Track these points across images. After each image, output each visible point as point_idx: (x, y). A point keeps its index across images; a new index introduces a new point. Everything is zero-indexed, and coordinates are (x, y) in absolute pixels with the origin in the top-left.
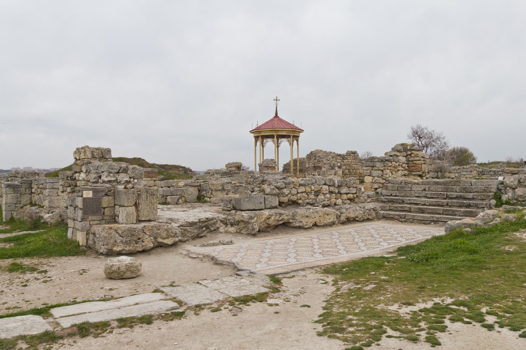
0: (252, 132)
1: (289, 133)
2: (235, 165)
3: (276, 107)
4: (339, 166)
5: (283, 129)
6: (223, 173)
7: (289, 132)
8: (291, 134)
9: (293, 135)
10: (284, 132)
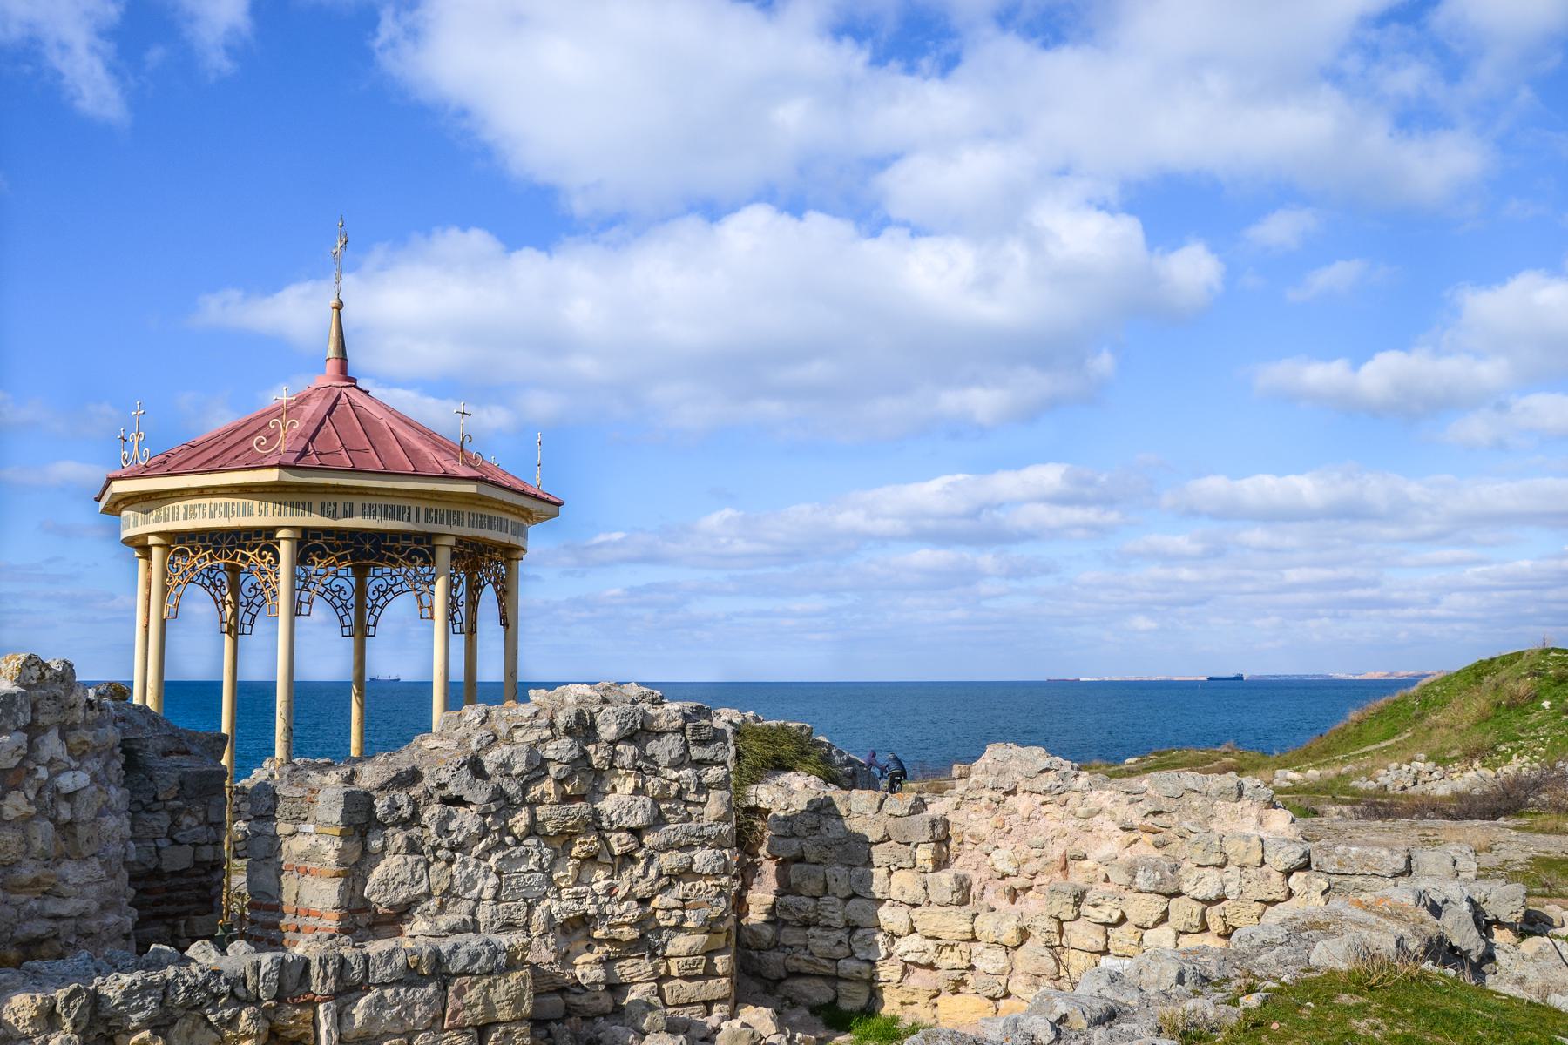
9: (460, 540)
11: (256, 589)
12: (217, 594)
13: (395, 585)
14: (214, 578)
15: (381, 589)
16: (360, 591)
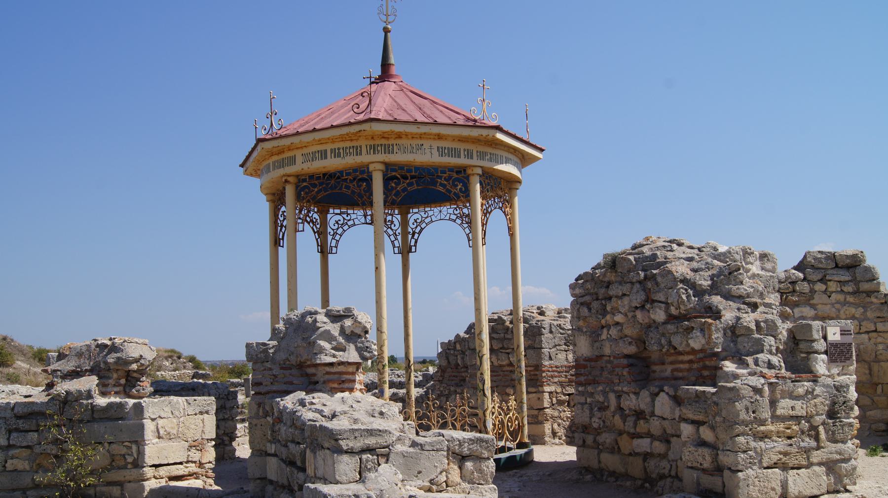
1: (456, 153)
3: (386, 31)
4: (835, 345)
5: (424, 129)
6: (18, 417)
7: (462, 146)
8: (475, 162)
10: (427, 144)
11: (338, 224)
12: (314, 227)
13: (427, 217)
14: (312, 216)
15: (418, 221)
16: (404, 223)
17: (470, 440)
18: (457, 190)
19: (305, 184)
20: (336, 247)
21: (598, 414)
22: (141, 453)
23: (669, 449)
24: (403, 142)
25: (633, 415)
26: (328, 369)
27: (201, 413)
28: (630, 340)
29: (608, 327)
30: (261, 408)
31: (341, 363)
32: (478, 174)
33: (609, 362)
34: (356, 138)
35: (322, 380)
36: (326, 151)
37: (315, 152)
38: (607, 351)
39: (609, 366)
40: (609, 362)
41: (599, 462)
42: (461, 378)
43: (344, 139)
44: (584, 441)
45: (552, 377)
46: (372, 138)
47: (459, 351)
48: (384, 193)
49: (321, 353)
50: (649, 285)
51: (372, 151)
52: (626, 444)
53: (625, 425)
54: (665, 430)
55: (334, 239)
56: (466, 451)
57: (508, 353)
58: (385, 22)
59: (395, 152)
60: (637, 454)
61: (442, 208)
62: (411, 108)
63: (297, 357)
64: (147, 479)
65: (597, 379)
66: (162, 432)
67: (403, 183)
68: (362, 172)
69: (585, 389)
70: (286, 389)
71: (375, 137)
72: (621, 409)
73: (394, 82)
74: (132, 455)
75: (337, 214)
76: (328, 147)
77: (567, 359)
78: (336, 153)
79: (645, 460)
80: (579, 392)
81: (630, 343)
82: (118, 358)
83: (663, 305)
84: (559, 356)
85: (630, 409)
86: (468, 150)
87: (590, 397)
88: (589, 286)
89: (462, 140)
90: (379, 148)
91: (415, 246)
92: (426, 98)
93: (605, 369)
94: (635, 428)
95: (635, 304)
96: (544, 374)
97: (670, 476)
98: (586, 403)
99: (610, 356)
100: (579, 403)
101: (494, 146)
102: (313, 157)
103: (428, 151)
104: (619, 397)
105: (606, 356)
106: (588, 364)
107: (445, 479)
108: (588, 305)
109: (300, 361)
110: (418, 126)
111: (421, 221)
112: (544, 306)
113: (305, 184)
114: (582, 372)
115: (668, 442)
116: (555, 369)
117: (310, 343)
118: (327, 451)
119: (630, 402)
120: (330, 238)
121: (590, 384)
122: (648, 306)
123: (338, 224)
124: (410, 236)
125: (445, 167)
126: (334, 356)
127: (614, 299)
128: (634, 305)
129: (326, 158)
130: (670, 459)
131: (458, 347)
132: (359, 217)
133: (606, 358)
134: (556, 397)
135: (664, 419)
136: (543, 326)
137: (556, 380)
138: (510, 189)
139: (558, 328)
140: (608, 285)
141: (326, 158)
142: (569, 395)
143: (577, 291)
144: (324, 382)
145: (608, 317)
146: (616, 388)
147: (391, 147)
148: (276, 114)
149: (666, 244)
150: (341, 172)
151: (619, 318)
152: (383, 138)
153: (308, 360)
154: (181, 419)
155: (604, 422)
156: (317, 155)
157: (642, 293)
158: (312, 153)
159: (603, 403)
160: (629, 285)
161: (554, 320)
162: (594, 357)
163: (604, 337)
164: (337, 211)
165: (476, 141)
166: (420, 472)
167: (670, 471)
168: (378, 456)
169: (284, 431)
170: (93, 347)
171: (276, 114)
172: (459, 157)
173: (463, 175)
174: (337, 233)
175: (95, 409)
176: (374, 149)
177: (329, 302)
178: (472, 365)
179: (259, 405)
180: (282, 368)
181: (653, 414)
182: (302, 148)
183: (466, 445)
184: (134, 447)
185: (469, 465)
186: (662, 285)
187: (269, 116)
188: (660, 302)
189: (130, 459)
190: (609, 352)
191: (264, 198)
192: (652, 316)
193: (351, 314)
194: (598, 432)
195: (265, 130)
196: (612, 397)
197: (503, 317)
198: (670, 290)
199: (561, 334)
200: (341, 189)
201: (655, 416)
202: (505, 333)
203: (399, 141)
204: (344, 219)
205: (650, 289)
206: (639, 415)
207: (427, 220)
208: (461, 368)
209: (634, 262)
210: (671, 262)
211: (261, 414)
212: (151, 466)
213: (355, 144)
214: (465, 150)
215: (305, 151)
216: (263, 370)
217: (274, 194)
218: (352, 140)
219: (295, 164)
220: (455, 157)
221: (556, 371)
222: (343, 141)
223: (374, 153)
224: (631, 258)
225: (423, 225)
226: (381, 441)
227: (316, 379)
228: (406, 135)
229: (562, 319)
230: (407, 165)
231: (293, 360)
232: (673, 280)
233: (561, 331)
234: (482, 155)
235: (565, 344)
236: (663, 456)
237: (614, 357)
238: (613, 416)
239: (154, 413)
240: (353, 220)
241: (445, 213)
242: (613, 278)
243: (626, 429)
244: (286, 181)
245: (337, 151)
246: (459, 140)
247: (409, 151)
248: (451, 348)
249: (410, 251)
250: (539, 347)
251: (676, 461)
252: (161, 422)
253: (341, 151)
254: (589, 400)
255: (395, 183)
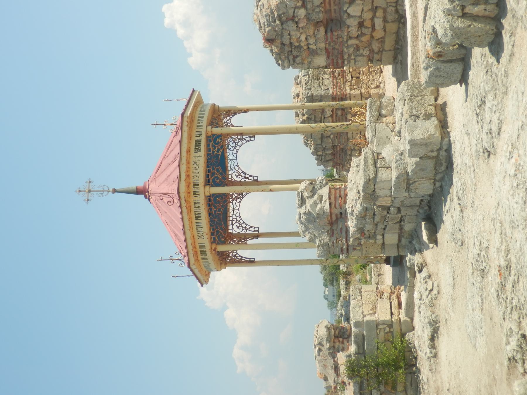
0: (202, 280)
1: (198, 142)
2: (325, 351)
3: (115, 191)
5: (184, 160)
7: (194, 138)
8: (203, 130)
10: (192, 160)
11: (239, 226)
15: (237, 175)
17: (370, 111)
18: (221, 142)
19: (217, 238)
20: (254, 228)
21: (361, 51)
22: (384, 323)
23: (380, 7)
24: (191, 174)
25: (361, 29)
26: (333, 206)
27: (360, 292)
28: (316, 31)
29: (308, 44)
30: (356, 248)
31: (330, 198)
32: (211, 129)
33: (329, 44)
34: (189, 203)
35: (339, 210)
36: (197, 223)
37: (197, 230)
38: (323, 45)
39: (332, 44)
40: (329, 44)
41: (390, 50)
42: (341, 151)
43: (190, 211)
44: (378, 60)
45: (340, 88)
46: (189, 193)
47: (322, 153)
48: (224, 186)
49: (323, 209)
50: (284, 19)
51: (197, 193)
52: (379, 34)
53: (367, 34)
54: (370, 10)
55: (249, 229)
56: (376, 113)
57: (324, 118)
58: (108, 192)
59: (198, 179)
60: (384, 26)
61: (228, 159)
62: (168, 172)
63: (326, 225)
64: (400, 319)
65: (340, 52)
66: (371, 312)
67: (217, 174)
68: (210, 200)
69: (346, 60)
70: (345, 232)
71: (189, 191)
72: (357, 37)
73: (149, 185)
74: (385, 329)
75: (233, 227)
76: (194, 221)
77: (328, 79)
78: (198, 216)
79: (388, 22)
80: (348, 63)
81: (318, 31)
82: (327, 340)
83: (296, 10)
84: (326, 83)
85: (358, 31)
86: (196, 134)
87: (351, 57)
88: (283, 56)
89: (190, 138)
90: (196, 189)
91: (253, 177)
92: (161, 163)
93: (334, 47)
94: (369, 28)
95: (295, 27)
96: (338, 93)
97: (396, 6)
98: (355, 59)
99: (326, 44)
100: (355, 63)
101: (193, 119)
102: (200, 231)
103: (197, 159)
104: (351, 38)
105: (326, 46)
106: (331, 58)
107: (391, 124)
108: (295, 57)
109: (328, 224)
110: (182, 164)
111: (237, 172)
112: (293, 94)
113: (217, 238)
114: (336, 61)
115: (376, 7)
116: (335, 87)
117: (318, 217)
118: (376, 186)
119: (354, 31)
120: (248, 232)
121: (343, 56)
122: (296, 20)
123: (239, 226)
124: (247, 180)
125: (207, 149)
126: (325, 201)
127: (292, 41)
128: (296, 28)
129: (201, 223)
130: (386, 6)
131: (320, 153)
132: (235, 213)
133: (327, 46)
134: (354, 86)
135: (363, 10)
136: (306, 94)
137: (342, 86)
138: (219, 111)
139: (308, 84)
140: (283, 44)
141: (201, 223)
142: (352, 77)
143: (286, 64)
144: (341, 208)
145: (302, 44)
146: (345, 40)
147: (194, 181)
148: (172, 257)
149: (259, 9)
150: (210, 214)
151: (303, 38)
152: (189, 186)
153: (328, 219)
154: (364, 302)
155: (366, 48)
156: (199, 229)
157: (289, 23)
158: (198, 232)
159: (354, 48)
160: (284, 31)
161: (302, 87)
162: (326, 54)
163: (314, 47)
164: (231, 227)
165: (190, 128)
166: (387, 137)
167: (393, 6)
168: (378, 159)
169: (369, 227)
170: (320, 358)
171: (172, 257)
172: (201, 140)
173: (212, 138)
174: (245, 227)
175: (357, 352)
176: (196, 192)
177: (290, 232)
178: (332, 142)
179: (354, 249)
180: (333, 236)
181: (360, 17)
182: (194, 239)
183: (373, 113)
184: (380, 327)
185: (384, 112)
186: (285, 11)
187: (173, 262)
188: (294, 12)
189: (388, 330)
190: (323, 44)
191: (223, 270)
192: (303, 17)
193: (301, 192)
194: (372, 51)
195: (181, 264)
196: (350, 42)
197: (300, 121)
198: (288, 6)
199: (312, 82)
200: (220, 214)
201: (361, 15)
202: (311, 120)
203: (191, 176)
204: (236, 223)
205: (286, 18)
206: (361, 25)
207: (237, 169)
208: (334, 151)
209: (270, 28)
210: (270, 6)
211: (359, 248)
212: (392, 317)
213: (192, 204)
214: (196, 136)
215: (196, 237)
216: (334, 247)
217: (221, 264)
218: (190, 206)
219: (204, 244)
220: (201, 142)
221: (336, 86)
222: (190, 212)
223: (198, 192)
224: (267, 30)
225: (240, 171)
226: (370, 157)
227: (339, 214)
228: (188, 172)
229: (302, 82)
230: (206, 172)
231: (328, 228)
232: (281, 4)
233: (310, 82)
234: (199, 126)
235: (319, 80)
236: (385, 11)
237: (327, 41)
238: (362, 41)
239: (360, 316)
240: (236, 217)
241: (232, 156)
242: (279, 41)
243: (369, 33)
244: (215, 250)
245: (197, 216)
246: (190, 139)
247: (197, 170)
248: (320, 159)
249: (257, 180)
250: (320, 97)
251: (387, 3)
252: (365, 313)
253: (197, 213)
254: (353, 57)
255: (217, 179)
